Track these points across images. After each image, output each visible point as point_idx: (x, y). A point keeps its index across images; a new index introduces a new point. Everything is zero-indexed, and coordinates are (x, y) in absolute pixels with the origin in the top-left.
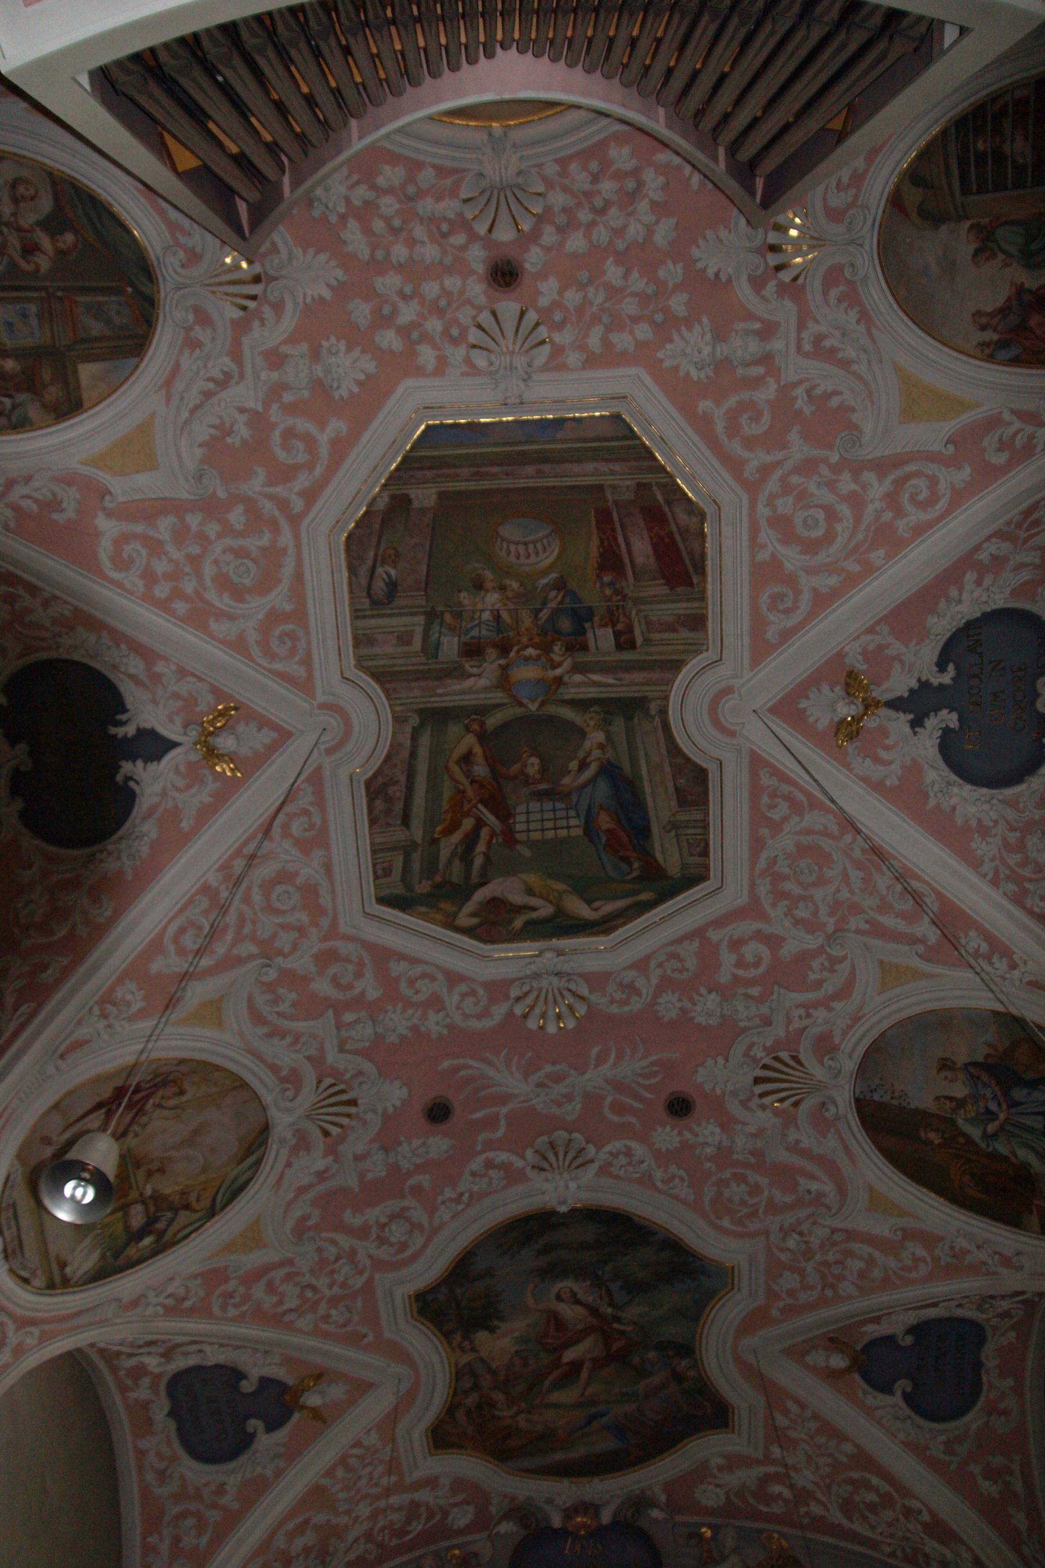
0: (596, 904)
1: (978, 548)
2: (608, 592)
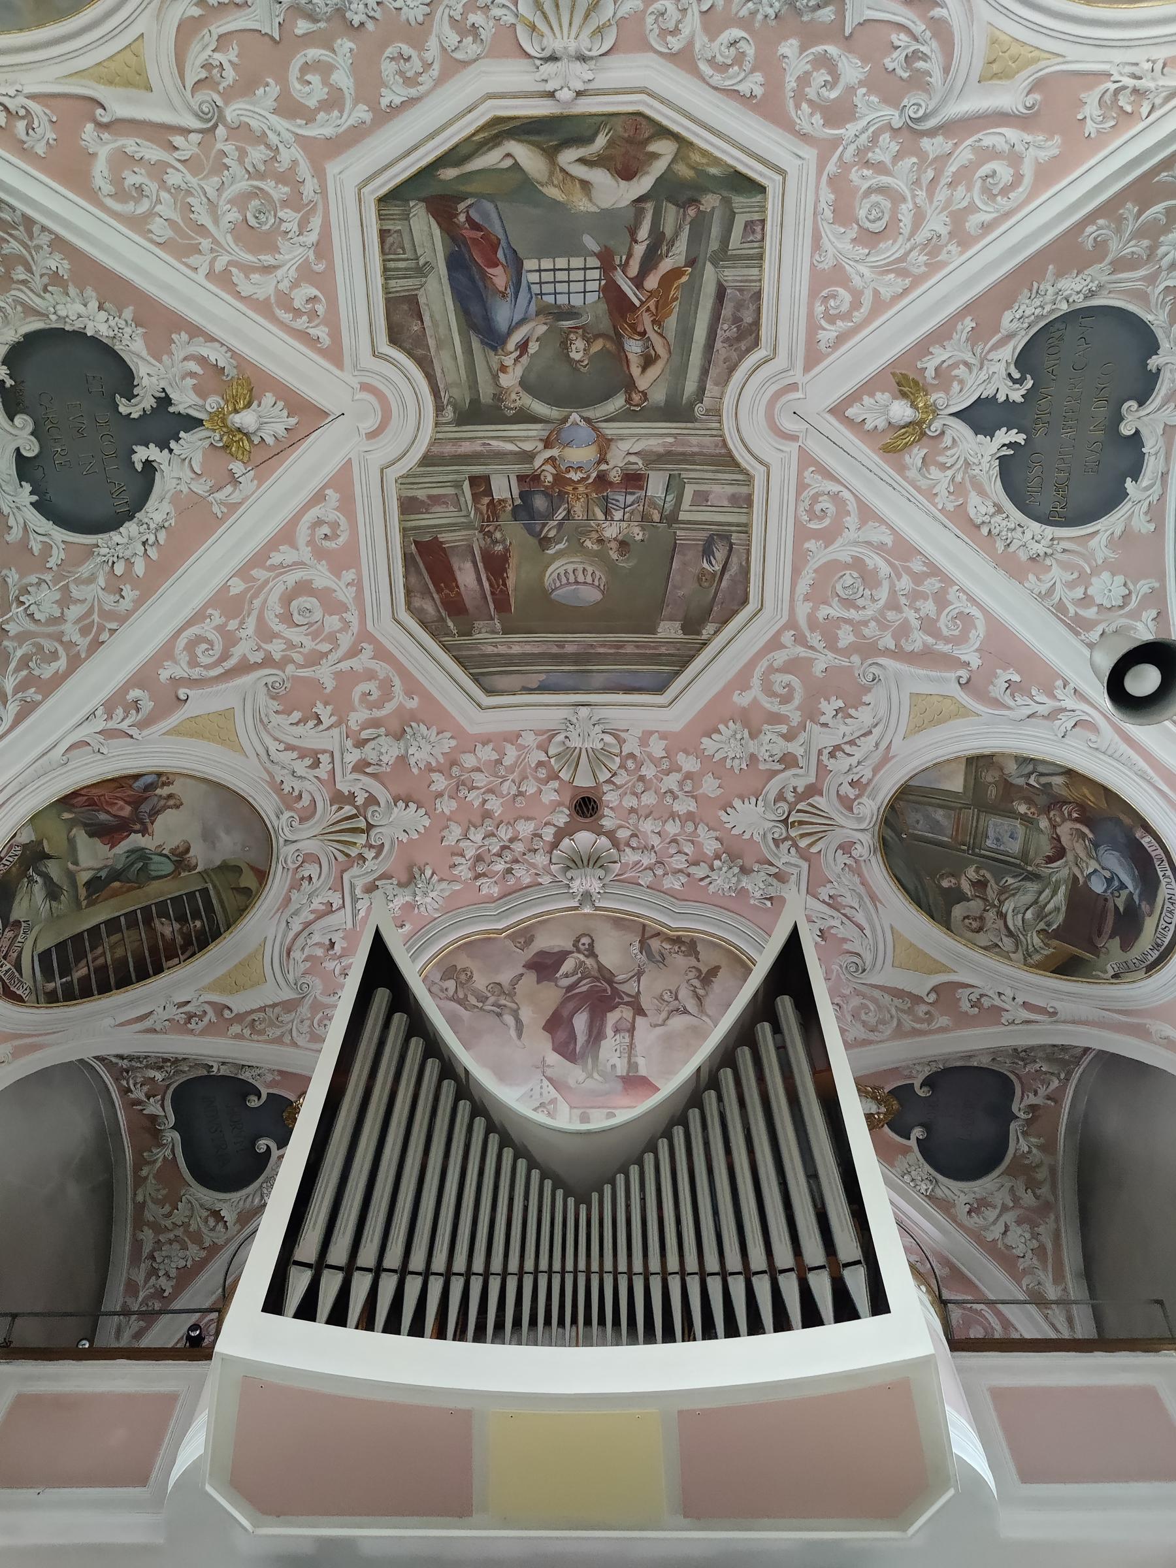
0: (508, 163)
1: (139, 603)
2: (498, 535)
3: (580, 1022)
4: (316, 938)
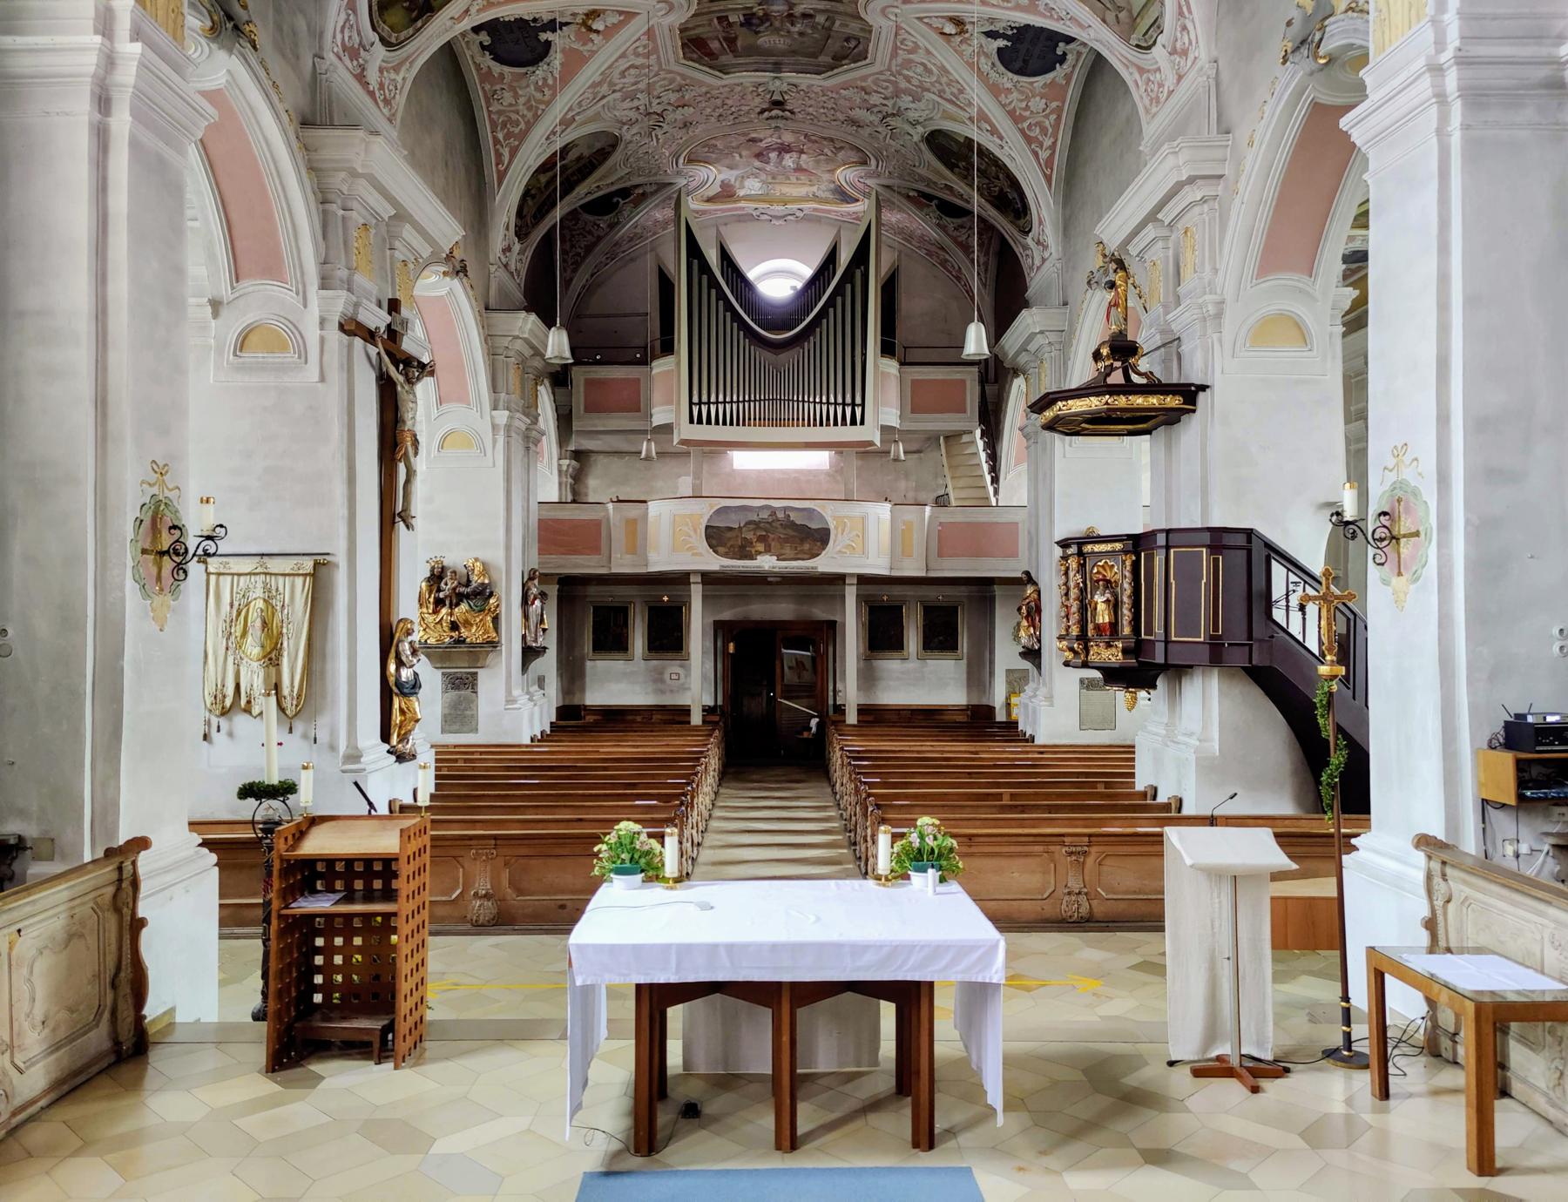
3: (773, 155)
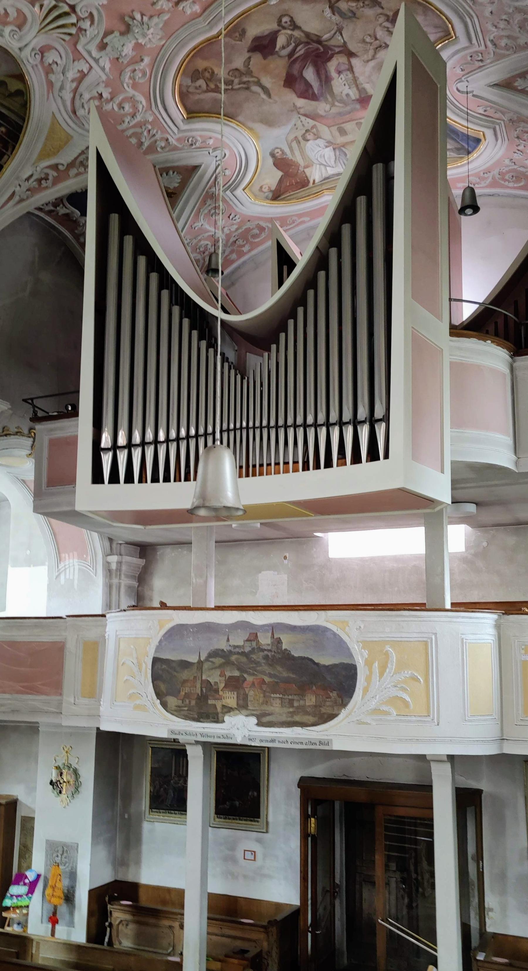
4: (87, 96)
